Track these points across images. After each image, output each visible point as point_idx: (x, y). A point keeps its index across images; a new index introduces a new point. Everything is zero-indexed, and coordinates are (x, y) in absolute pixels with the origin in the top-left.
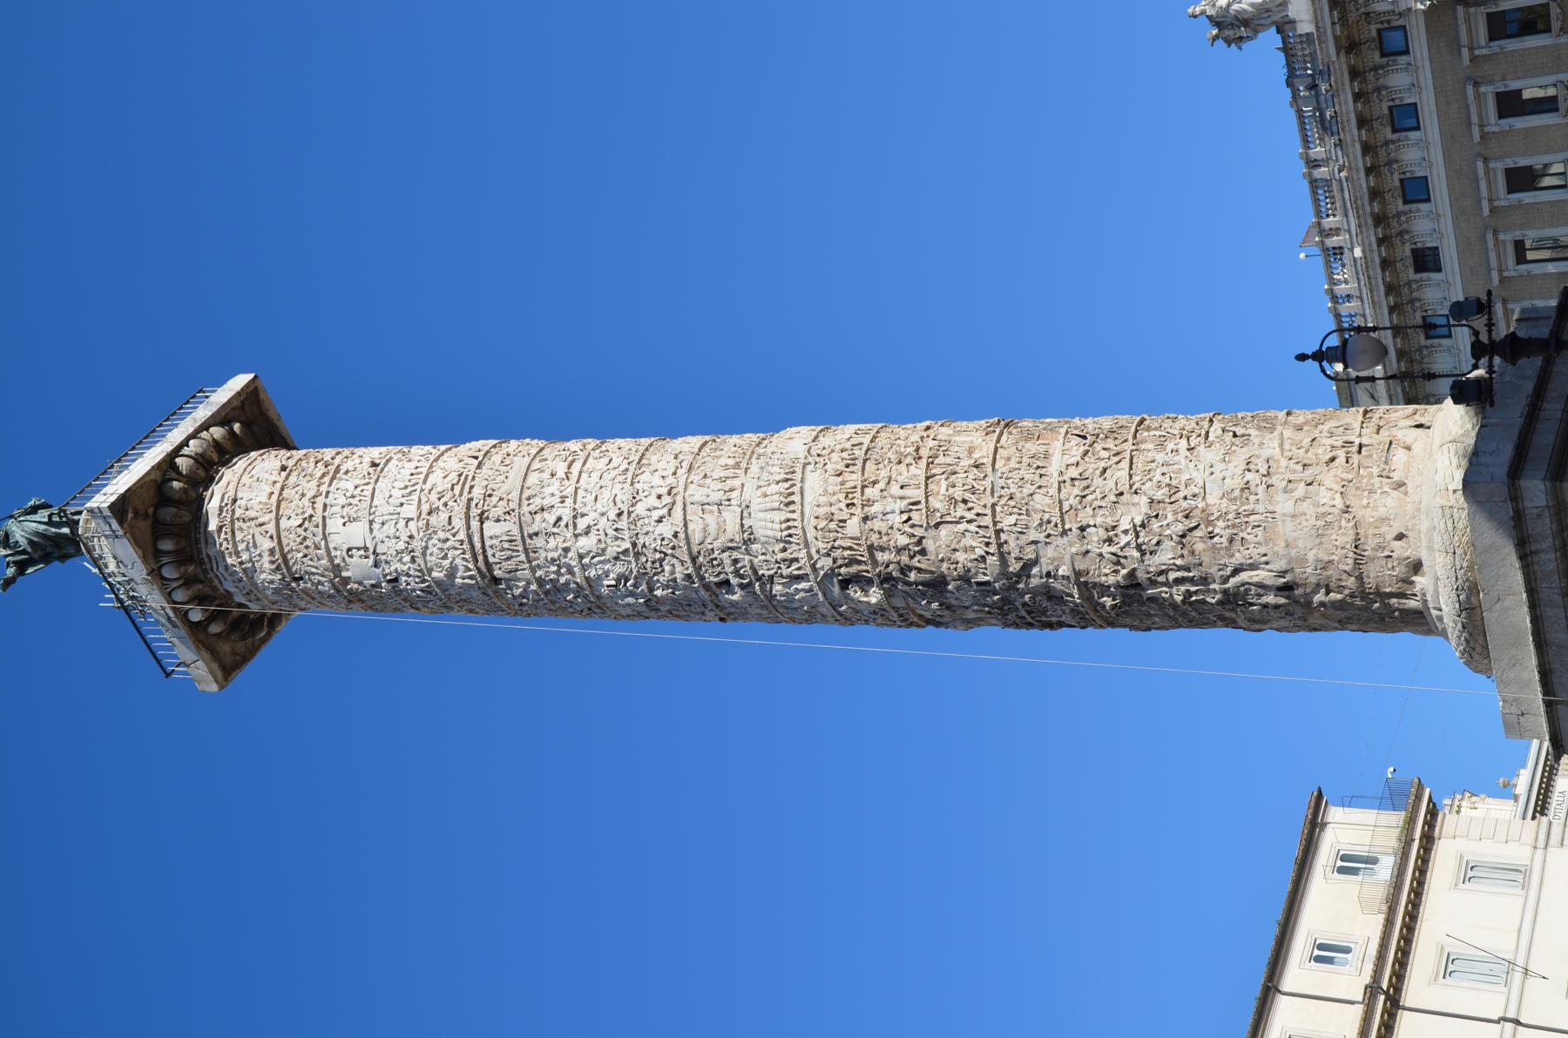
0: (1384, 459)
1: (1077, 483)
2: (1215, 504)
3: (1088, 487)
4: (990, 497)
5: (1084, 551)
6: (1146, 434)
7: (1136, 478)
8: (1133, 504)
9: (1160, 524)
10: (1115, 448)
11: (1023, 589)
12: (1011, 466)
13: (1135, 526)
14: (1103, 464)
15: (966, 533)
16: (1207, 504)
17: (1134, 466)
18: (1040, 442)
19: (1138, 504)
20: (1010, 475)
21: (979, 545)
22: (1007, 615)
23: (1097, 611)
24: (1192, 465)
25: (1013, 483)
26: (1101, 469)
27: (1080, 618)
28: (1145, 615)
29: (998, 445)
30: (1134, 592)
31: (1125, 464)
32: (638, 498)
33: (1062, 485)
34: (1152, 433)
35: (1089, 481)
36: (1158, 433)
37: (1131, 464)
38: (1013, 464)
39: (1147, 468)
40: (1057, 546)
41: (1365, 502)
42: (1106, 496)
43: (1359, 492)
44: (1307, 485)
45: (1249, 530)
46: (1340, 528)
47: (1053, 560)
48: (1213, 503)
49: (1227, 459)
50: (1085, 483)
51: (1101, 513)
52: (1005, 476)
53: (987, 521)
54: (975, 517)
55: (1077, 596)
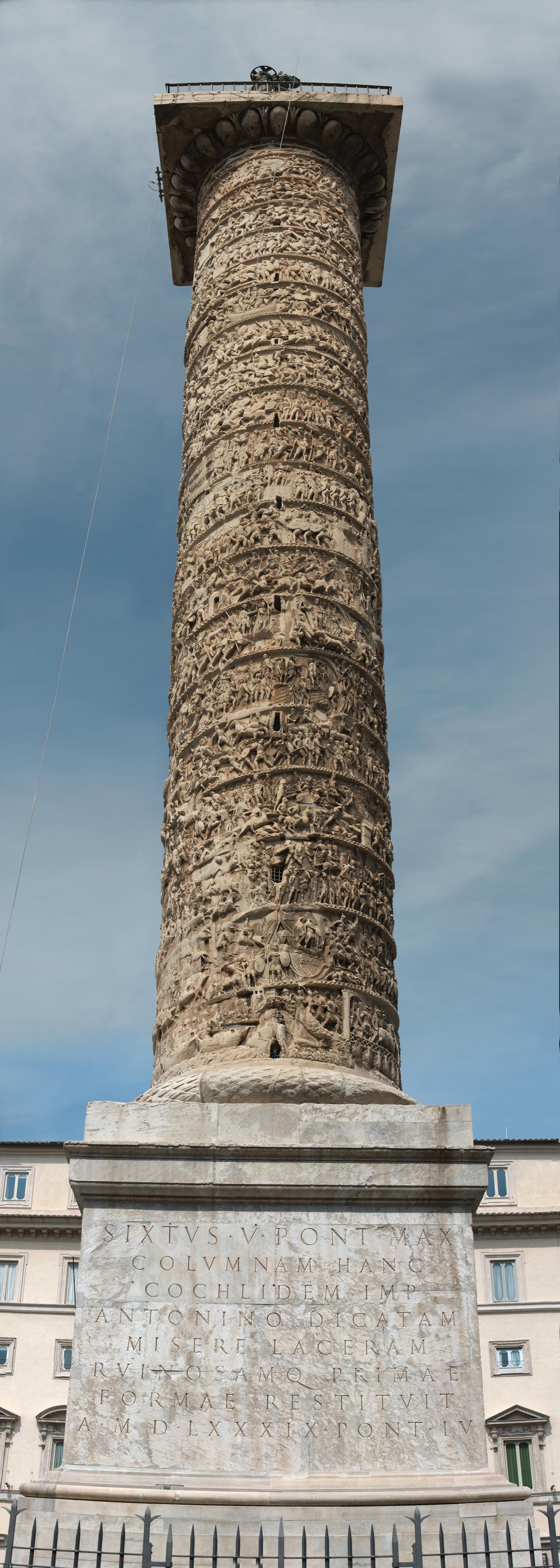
0: (230, 1022)
2: (191, 881)
16: (191, 873)
32: (221, 410)
44: (202, 959)
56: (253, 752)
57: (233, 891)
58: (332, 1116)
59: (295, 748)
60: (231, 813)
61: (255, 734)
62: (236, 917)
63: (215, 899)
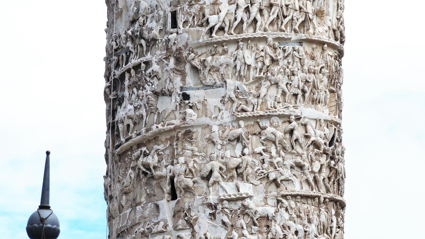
1: (288, 136)
3: (284, 148)
4: (275, 36)
5: (215, 140)
6: (333, 212)
7: (293, 203)
8: (266, 198)
9: (245, 227)
10: (322, 178)
11: (167, 65)
12: (306, 61)
13: (243, 199)
14: (307, 165)
15: (234, 6)
17: (304, 201)
18: (328, 92)
19: (266, 204)
20: (297, 60)
21: (221, 20)
22: (133, 41)
23: (139, 145)
25: (289, 63)
26: (303, 163)
27: (128, 126)
28: (134, 200)
29: (326, 46)
30: (165, 190)
31: (306, 190)
33: (286, 119)
34: (334, 218)
35: (290, 150)
36: (334, 225)
37: (307, 197)
38: (308, 62)
39: (302, 215)
40: (220, 110)
42: (275, 168)
47: (204, 103)
50: (288, 146)
51: (257, 162)
52: (296, 53)
53: (249, 33)
54: (252, 18)
55: (160, 127)
60: (305, 232)
61: (323, 147)
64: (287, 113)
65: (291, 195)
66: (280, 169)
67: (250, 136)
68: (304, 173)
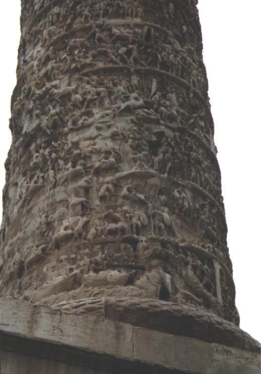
0: (116, 263)
7: (95, 77)
16: (67, 134)
24: (109, 112)
41: (63, 257)
43: (74, 250)
45: (42, 175)
46: (37, 246)
48: (68, 138)
49: (118, 137)
56: (129, 53)
57: (115, 152)
58: (243, 361)
59: (162, 58)
61: (131, 39)
62: (118, 175)
63: (94, 158)
64: (87, 25)
65: (91, 71)
66: (81, 60)
67: (57, 52)
68: (109, 57)
